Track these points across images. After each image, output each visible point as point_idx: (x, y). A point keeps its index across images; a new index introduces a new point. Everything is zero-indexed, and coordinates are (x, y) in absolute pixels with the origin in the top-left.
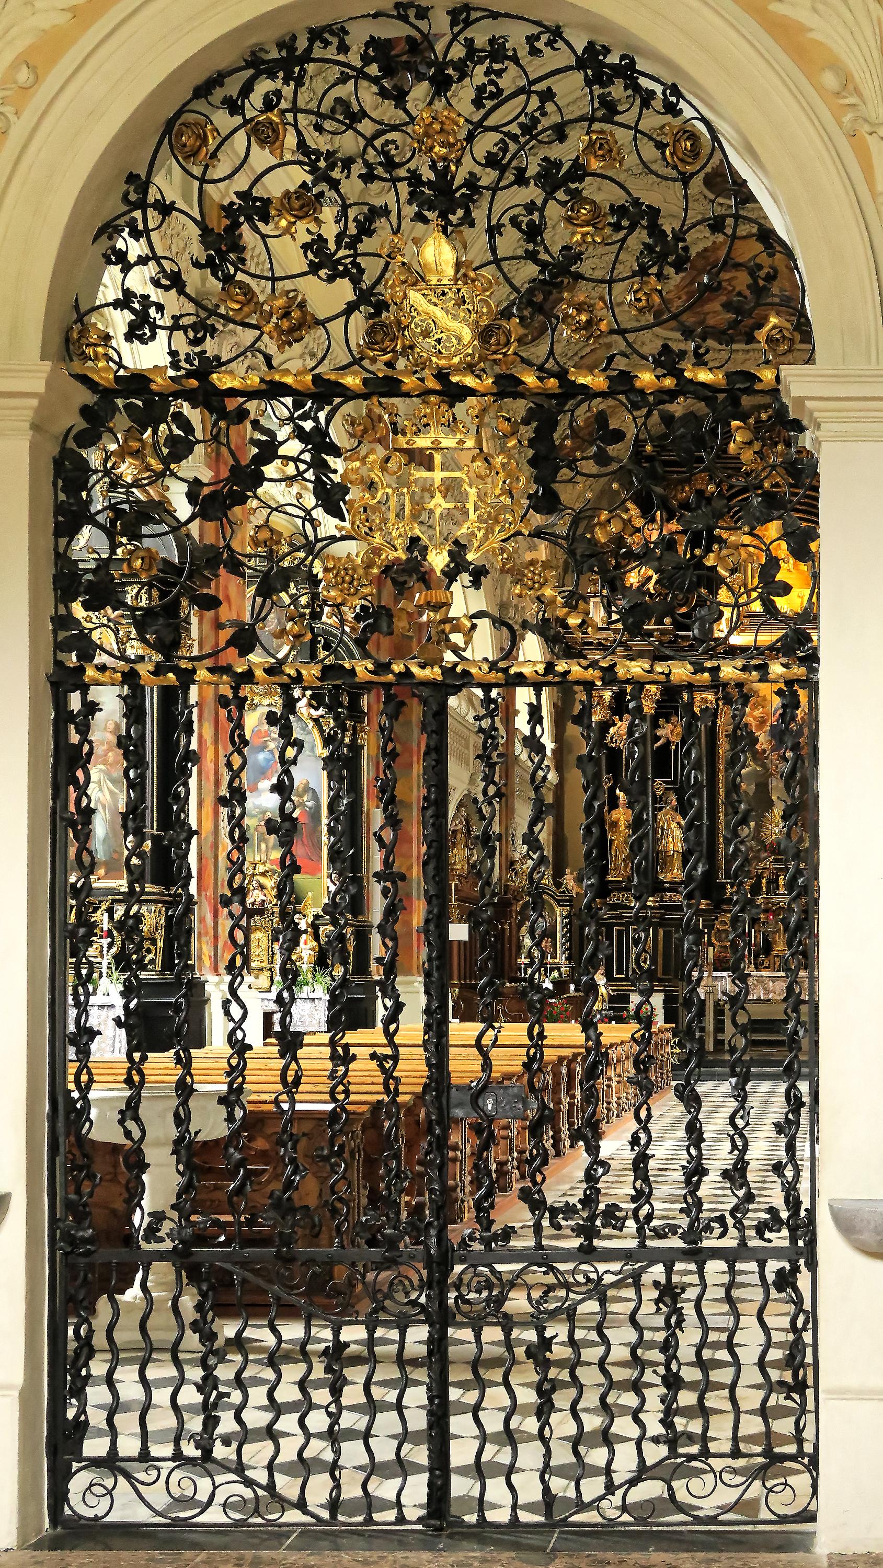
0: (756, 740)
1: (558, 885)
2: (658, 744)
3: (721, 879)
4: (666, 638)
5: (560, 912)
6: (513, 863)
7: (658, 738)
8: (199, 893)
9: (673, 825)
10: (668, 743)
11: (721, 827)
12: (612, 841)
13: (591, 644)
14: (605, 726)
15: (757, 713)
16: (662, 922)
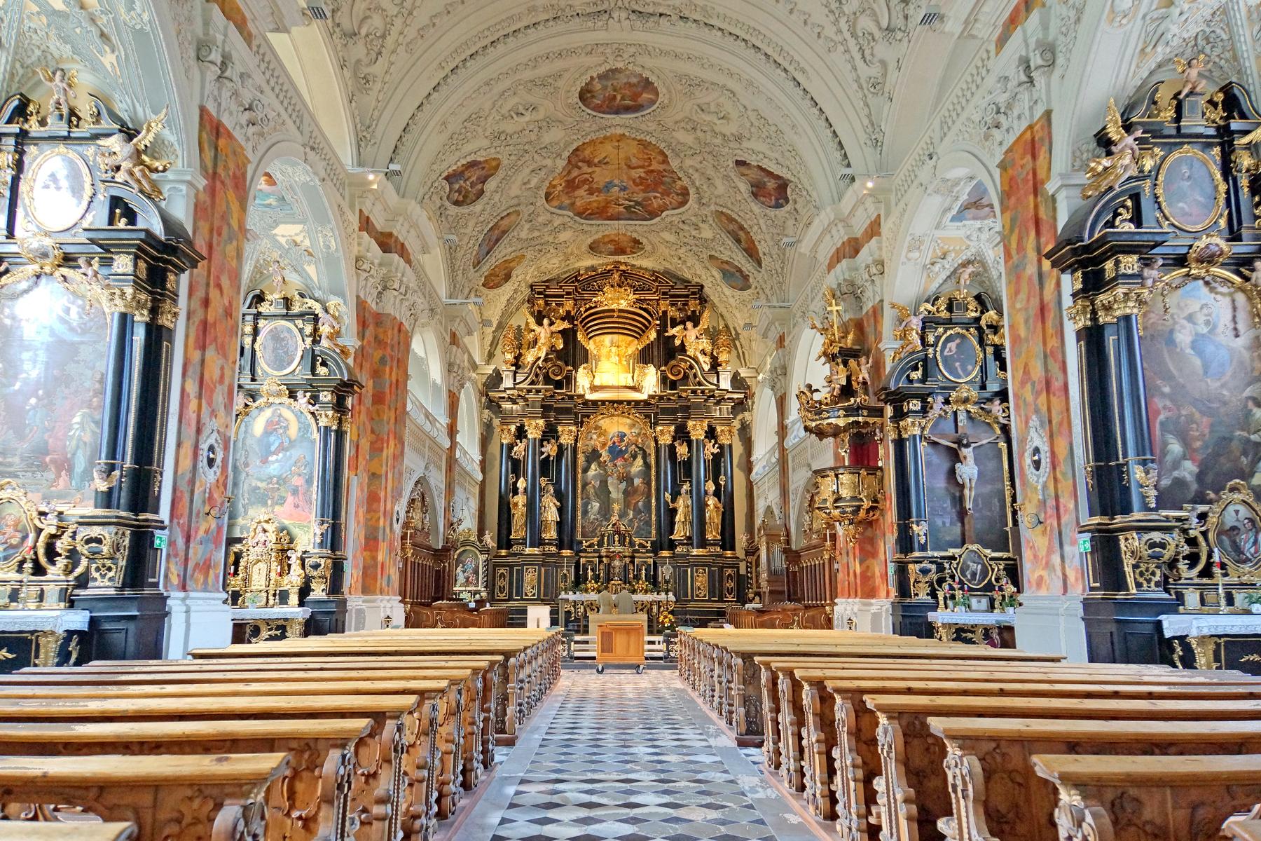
1: (481, 541)
3: (579, 538)
4: (548, 394)
5: (482, 558)
8: (171, 521)
10: (549, 456)
14: (511, 447)
15: (601, 439)
16: (544, 564)
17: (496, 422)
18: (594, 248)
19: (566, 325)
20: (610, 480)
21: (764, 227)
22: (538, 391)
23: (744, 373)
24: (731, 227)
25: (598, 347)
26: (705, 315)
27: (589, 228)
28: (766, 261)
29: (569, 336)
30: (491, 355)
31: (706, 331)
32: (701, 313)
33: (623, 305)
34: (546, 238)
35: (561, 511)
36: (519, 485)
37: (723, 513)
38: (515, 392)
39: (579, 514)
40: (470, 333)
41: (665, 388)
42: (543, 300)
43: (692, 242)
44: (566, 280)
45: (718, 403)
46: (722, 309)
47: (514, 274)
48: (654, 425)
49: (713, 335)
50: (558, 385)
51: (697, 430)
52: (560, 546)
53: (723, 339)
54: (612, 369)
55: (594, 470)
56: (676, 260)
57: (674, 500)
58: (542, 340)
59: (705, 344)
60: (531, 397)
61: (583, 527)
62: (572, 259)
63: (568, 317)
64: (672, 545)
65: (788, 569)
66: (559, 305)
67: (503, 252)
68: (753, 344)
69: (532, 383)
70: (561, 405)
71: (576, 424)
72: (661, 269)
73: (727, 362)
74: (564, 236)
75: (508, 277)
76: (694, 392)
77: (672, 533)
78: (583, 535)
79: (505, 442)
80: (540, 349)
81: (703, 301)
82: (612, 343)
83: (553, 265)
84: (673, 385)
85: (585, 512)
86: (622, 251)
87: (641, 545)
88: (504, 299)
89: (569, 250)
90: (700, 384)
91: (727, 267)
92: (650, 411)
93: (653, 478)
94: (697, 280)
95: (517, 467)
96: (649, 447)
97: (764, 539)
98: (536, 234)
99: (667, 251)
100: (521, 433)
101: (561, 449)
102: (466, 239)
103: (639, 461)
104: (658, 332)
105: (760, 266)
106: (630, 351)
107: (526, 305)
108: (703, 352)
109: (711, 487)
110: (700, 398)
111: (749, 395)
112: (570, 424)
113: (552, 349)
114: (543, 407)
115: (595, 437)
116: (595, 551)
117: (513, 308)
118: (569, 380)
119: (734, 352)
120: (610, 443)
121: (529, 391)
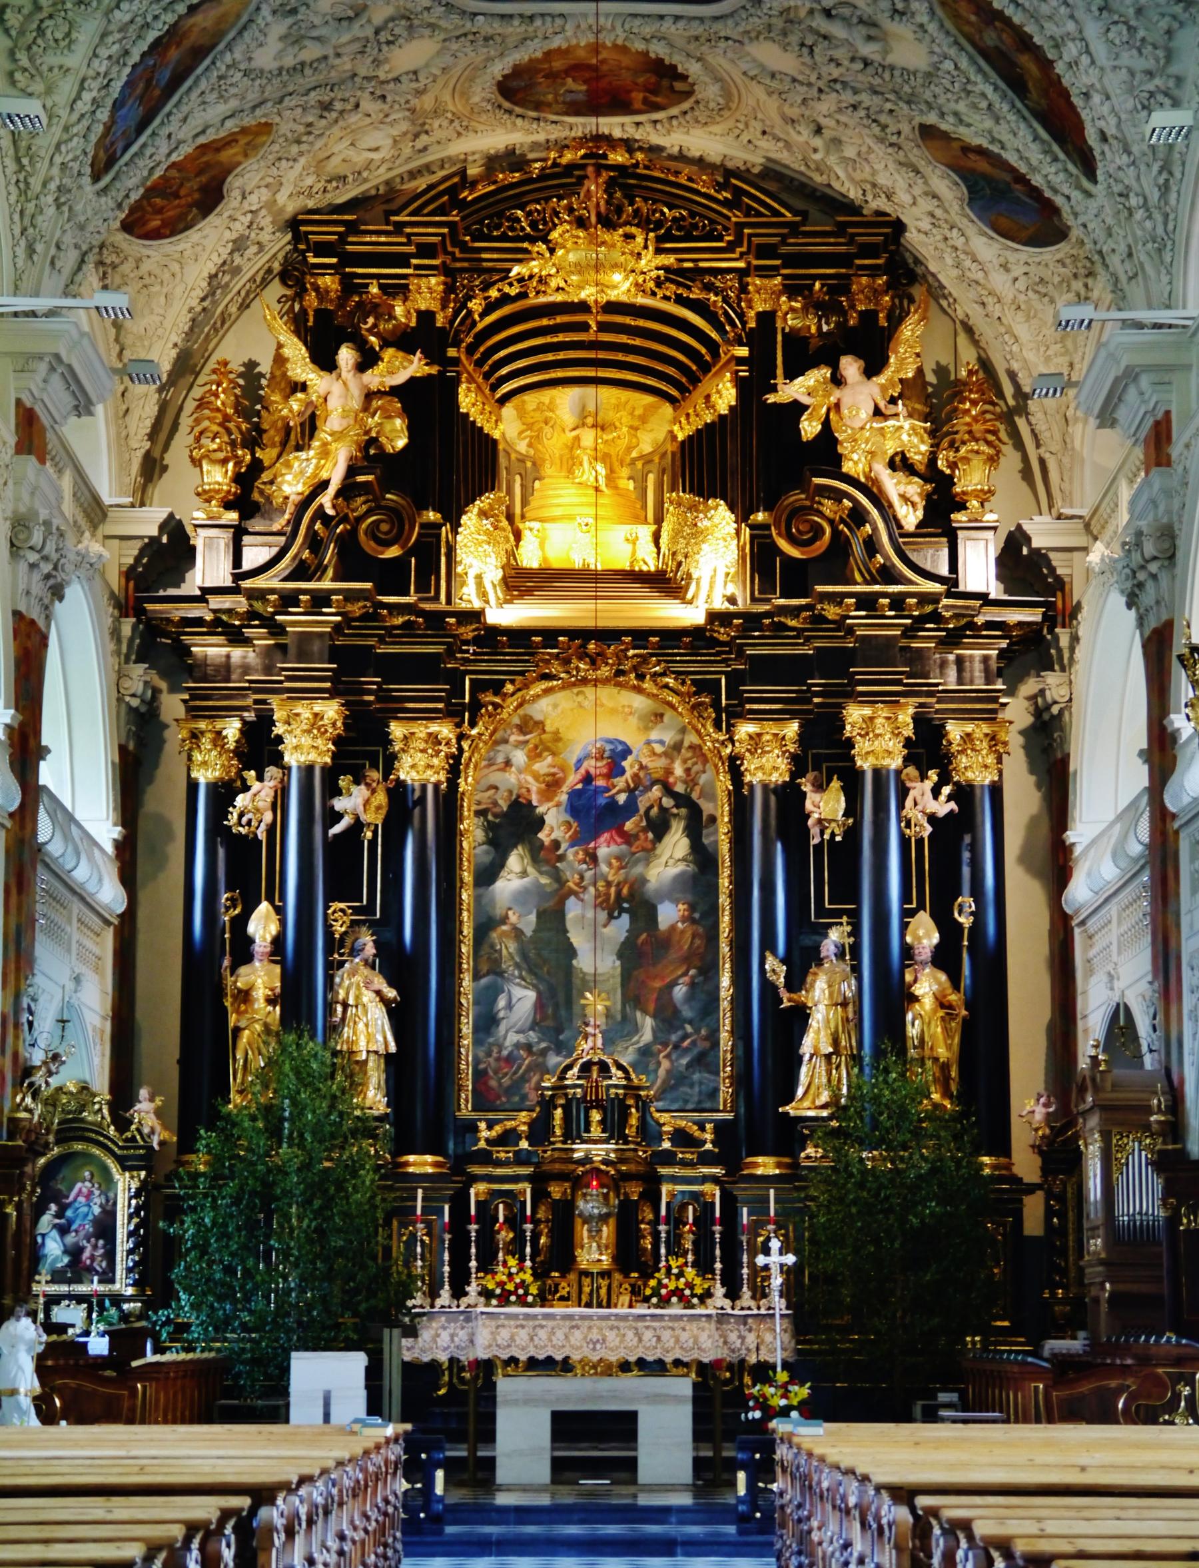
0: (540, 822)
1: (122, 1124)
2: (337, 829)
3: (465, 1110)
4: (356, 609)
5: (125, 1184)
6: (28, 1071)
7: (337, 817)
9: (368, 997)
10: (358, 826)
11: (466, 1001)
12: (237, 1031)
13: (199, 622)
14: (223, 794)
15: (543, 766)
17: (173, 705)
18: (518, 91)
19: (415, 367)
20: (573, 909)
21: (1100, 50)
22: (320, 600)
23: (1043, 533)
24: (990, 38)
25: (533, 429)
26: (909, 330)
27: (497, 27)
28: (1109, 160)
29: (426, 403)
30: (152, 468)
31: (913, 389)
32: (897, 320)
33: (620, 287)
34: (345, 64)
35: (402, 1016)
36: (253, 928)
37: (968, 1028)
38: (240, 603)
39: (467, 1028)
40: (83, 407)
41: (767, 586)
42: (333, 279)
43: (865, 79)
44: (420, 202)
45: (952, 640)
46: (966, 306)
47: (234, 184)
48: (727, 718)
49: (935, 401)
50: (391, 577)
51: (877, 735)
52: (404, 1145)
53: (971, 410)
54: (583, 511)
55: (516, 877)
56: (802, 136)
58: (333, 422)
59: (907, 434)
60: (296, 621)
61: (480, 1076)
62: (439, 128)
63: (421, 337)
64: (787, 1136)
65: (1173, 1221)
66: (400, 290)
67: (196, 117)
68: (1076, 430)
69: (301, 572)
70: (405, 654)
71: (453, 713)
72: (756, 160)
73: (985, 497)
74: (412, 54)
75: (210, 198)
76: (867, 602)
77: (789, 1097)
78: (483, 1101)
79: (203, 777)
80: (325, 453)
81: (905, 276)
82: (583, 415)
83: (368, 151)
84: (796, 579)
85: (487, 1023)
86: (618, 104)
87: (682, 1138)
88: (197, 275)
89: (428, 102)
90: (887, 575)
91: (983, 166)
92: (716, 668)
93: (724, 900)
94: (878, 203)
95: (244, 866)
96: (711, 796)
97: (1094, 1121)
98: (311, 52)
99: (772, 106)
100: (260, 748)
101: (402, 802)
102: (67, 88)
103: (676, 844)
104: (739, 383)
105: (1091, 174)
106: (647, 448)
107: (276, 289)
108: (900, 463)
109: (925, 934)
110: (890, 626)
111: (1061, 613)
112: (430, 716)
113: (370, 454)
114: (334, 654)
115: (519, 757)
116: (521, 1159)
117: (227, 302)
118: (431, 558)
119: (1010, 459)
120: (573, 780)
121: (288, 600)
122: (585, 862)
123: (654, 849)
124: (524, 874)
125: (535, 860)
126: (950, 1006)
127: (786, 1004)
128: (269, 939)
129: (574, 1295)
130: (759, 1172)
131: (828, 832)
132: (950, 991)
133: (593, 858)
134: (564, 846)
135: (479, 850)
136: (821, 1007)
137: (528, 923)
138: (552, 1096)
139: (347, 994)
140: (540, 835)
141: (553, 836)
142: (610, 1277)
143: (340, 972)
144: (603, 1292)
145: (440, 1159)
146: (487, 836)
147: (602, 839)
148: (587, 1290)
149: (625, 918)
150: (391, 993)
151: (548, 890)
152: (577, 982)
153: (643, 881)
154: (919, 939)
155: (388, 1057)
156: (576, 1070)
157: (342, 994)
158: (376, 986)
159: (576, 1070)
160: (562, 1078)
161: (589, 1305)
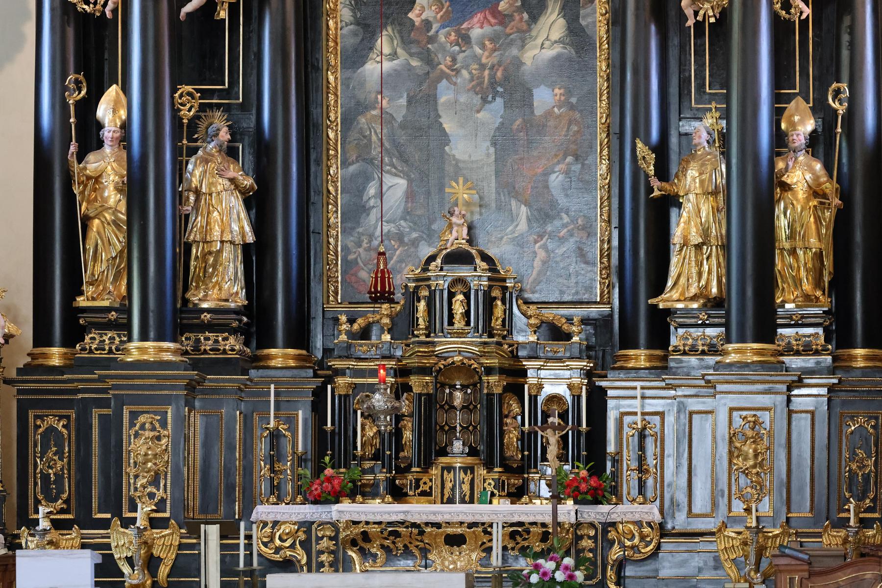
9: (222, 183)
12: (87, 219)
20: (445, 94)
55: (385, 59)
57: (663, 173)
122: (458, 44)
123: (529, 30)
124: (394, 55)
125: (406, 43)
126: (825, 196)
127: (656, 193)
128: (119, 124)
129: (436, 492)
130: (631, 364)
131: (702, 12)
132: (824, 179)
133: (464, 39)
134: (435, 27)
135: (346, 30)
136: (691, 197)
137: (397, 106)
138: (417, 287)
139: (201, 183)
140: (410, 15)
141: (423, 17)
142: (472, 472)
143: (193, 160)
144: (466, 488)
145: (304, 352)
146: (355, 16)
147: (475, 20)
148: (449, 485)
149: (499, 101)
150: (248, 182)
151: (420, 72)
152: (449, 169)
153: (518, 63)
154: (793, 125)
155: (246, 247)
156: (439, 261)
157: (195, 182)
158: (231, 174)
159: (439, 261)
160: (425, 269)
161: (451, 501)
